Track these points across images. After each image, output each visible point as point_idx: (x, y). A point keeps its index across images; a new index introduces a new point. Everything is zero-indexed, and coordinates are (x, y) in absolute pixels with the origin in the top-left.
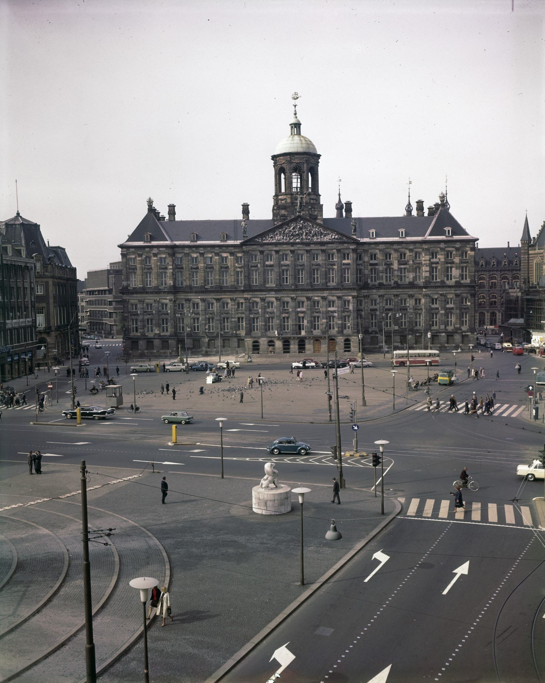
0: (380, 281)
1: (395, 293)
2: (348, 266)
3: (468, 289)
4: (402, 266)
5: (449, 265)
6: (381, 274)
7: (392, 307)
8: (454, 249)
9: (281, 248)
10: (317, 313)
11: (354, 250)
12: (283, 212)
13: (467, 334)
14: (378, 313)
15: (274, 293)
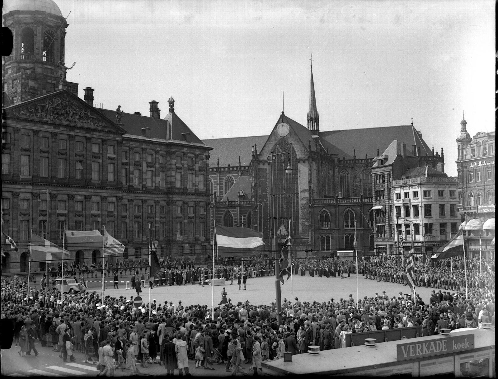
0: (130, 184)
1: (144, 198)
2: (113, 161)
3: (205, 197)
4: (149, 169)
5: (191, 172)
6: (131, 176)
7: (141, 214)
8: (194, 155)
9: (42, 129)
10: (79, 216)
11: (119, 143)
12: (32, 83)
13: (205, 244)
14: (127, 220)
15: (30, 187)
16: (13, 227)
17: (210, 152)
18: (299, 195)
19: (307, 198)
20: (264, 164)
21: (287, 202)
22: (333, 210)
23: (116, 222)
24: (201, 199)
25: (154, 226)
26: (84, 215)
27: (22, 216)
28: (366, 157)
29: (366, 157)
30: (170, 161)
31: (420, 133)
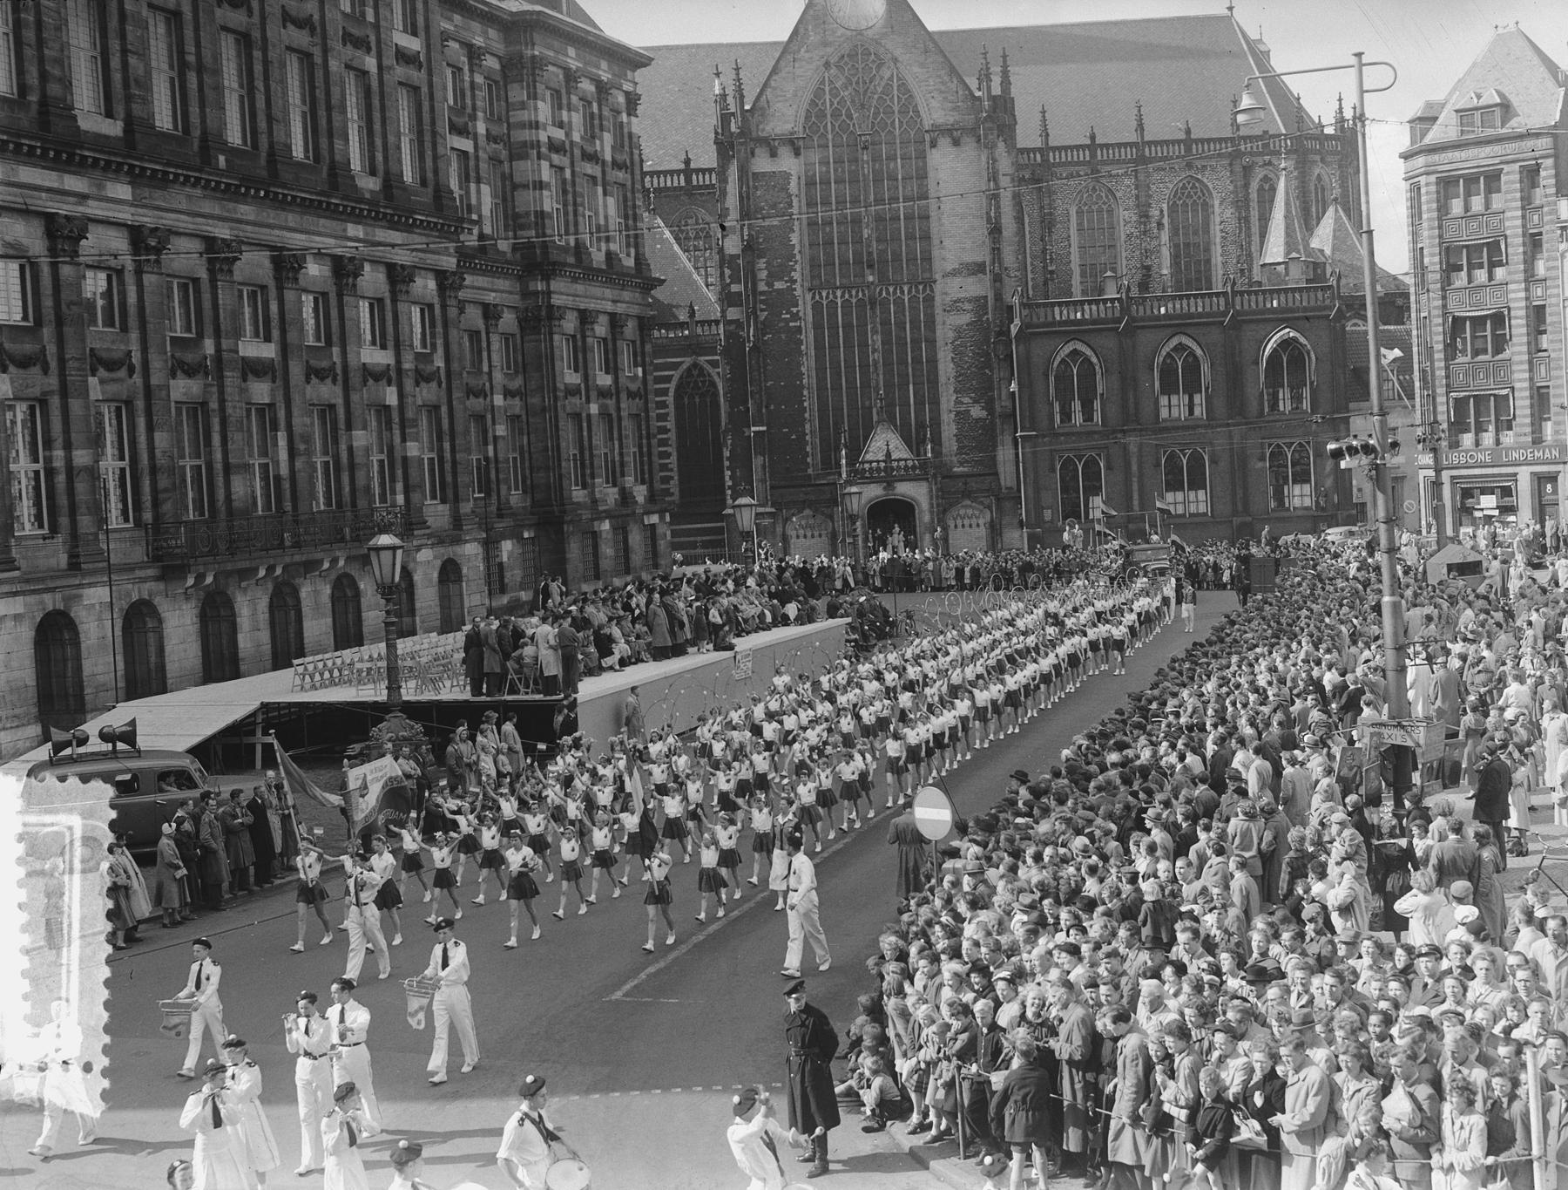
15: (123, 191)
16: (68, 446)
17: (640, 75)
18: (938, 288)
19: (977, 299)
20: (773, 154)
21: (885, 323)
22: (1110, 343)
23: (444, 409)
24: (626, 302)
25: (490, 434)
26: (339, 370)
27: (102, 372)
28: (1093, 137)
29: (1093, 137)
30: (523, 106)
31: (1262, 48)
